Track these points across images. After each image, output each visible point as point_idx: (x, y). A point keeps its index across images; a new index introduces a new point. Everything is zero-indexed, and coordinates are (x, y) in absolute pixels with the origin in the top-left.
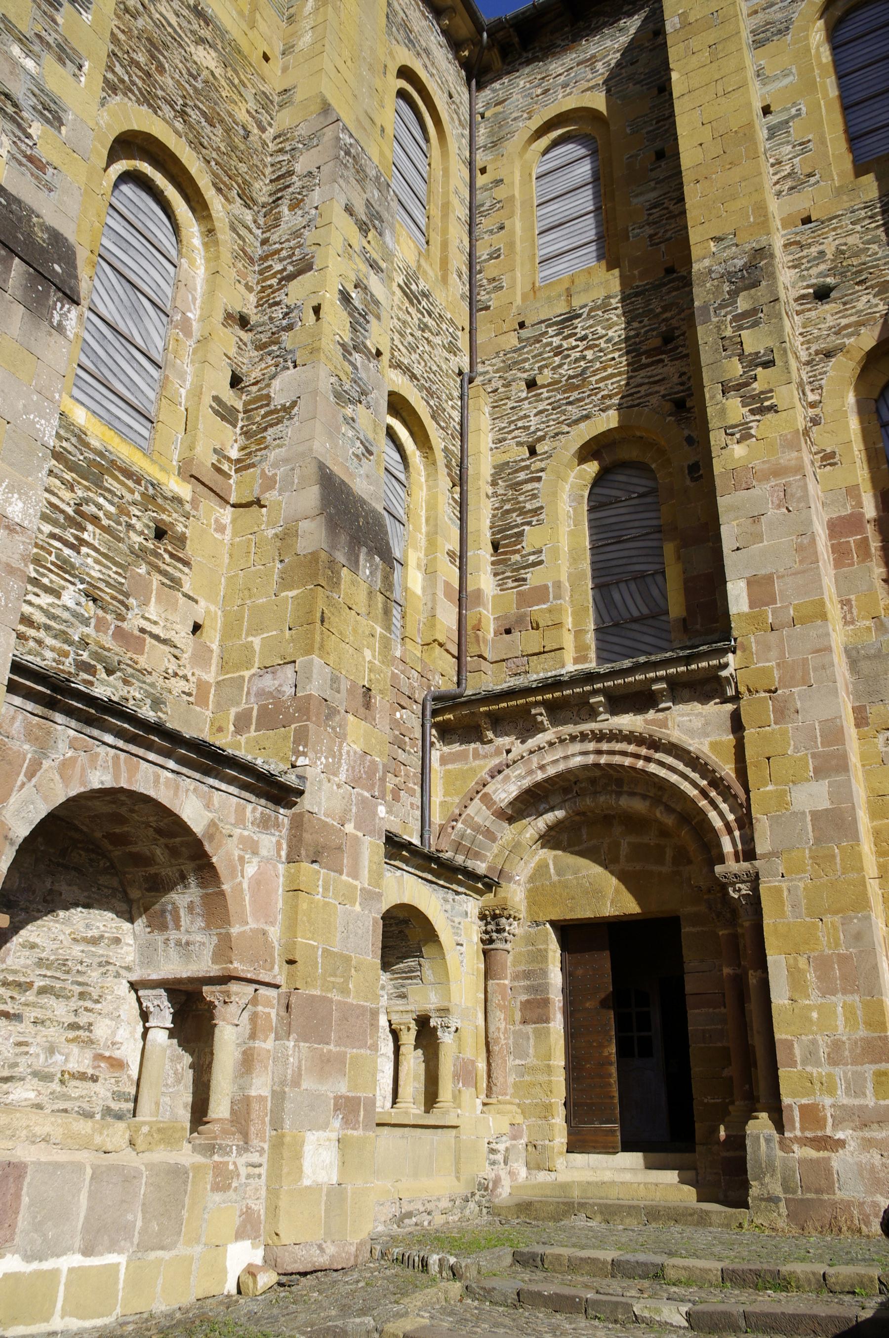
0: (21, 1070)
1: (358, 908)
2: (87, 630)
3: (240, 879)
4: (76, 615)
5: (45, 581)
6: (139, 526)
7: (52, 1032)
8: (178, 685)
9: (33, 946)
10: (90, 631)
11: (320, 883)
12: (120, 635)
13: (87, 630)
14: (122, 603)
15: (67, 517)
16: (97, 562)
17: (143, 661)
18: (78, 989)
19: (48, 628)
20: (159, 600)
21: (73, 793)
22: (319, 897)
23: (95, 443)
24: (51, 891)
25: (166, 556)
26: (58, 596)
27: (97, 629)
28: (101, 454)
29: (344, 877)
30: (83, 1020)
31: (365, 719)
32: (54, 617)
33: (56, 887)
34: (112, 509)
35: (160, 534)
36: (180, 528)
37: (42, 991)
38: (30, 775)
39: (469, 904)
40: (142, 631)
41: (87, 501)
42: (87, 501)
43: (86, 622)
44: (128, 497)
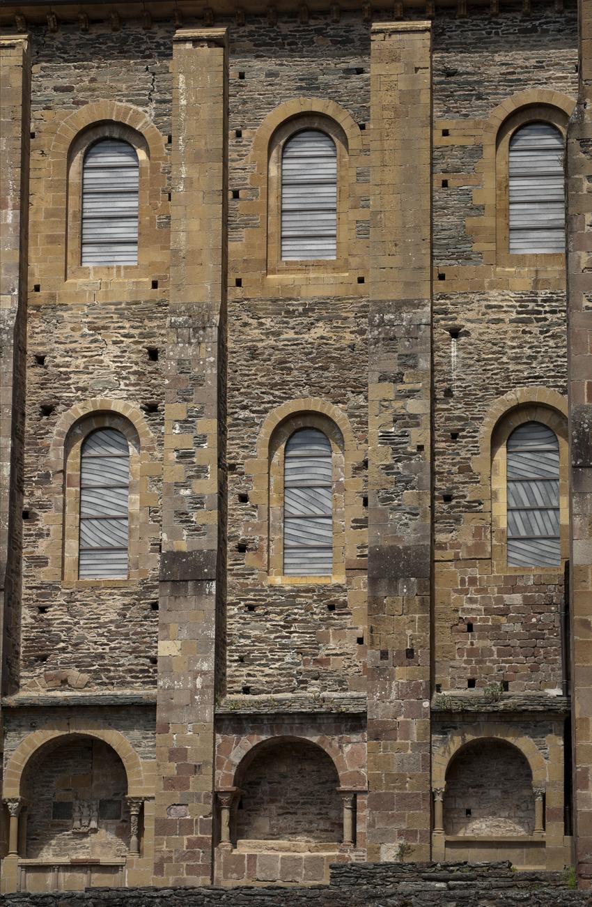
0: (299, 830)
1: (409, 752)
2: (299, 668)
4: (292, 663)
5: (276, 657)
6: (317, 611)
7: (311, 817)
8: (351, 671)
9: (297, 789)
10: (301, 667)
12: (316, 661)
13: (299, 668)
14: (315, 648)
15: (282, 626)
16: (298, 637)
17: (330, 668)
19: (281, 674)
20: (334, 638)
21: (255, 744)
23: (288, 588)
24: (301, 769)
25: (335, 617)
26: (283, 661)
27: (304, 665)
28: (292, 591)
29: (398, 741)
31: (410, 665)
32: (283, 669)
34: (303, 611)
35: (331, 607)
36: (342, 599)
37: (303, 804)
38: (237, 744)
39: (553, 725)
40: (328, 655)
41: (289, 615)
42: (289, 615)
43: (298, 664)
44: (310, 601)
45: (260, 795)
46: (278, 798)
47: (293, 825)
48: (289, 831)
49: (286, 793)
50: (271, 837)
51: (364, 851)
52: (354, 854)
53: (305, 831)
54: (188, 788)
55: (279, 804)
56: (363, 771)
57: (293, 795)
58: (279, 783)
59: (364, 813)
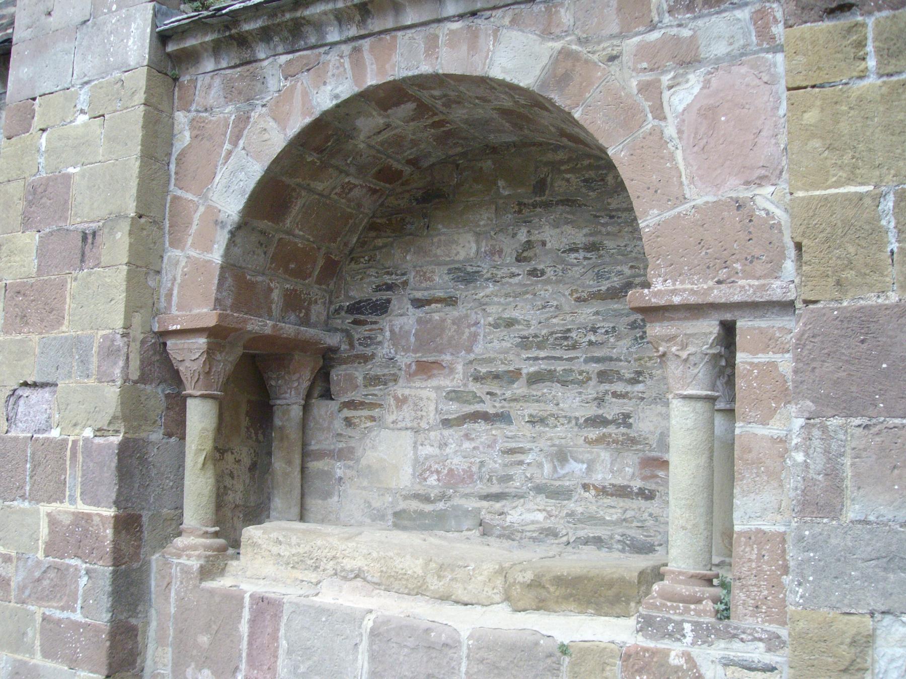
3: (651, 122)
7: (560, 433)
9: (510, 323)
11: (870, 48)
18: (595, 367)
22: (872, 80)
24: (529, 245)
30: (612, 410)
33: (536, 237)
37: (535, 379)
45: (385, 350)
46: (447, 358)
47: (495, 462)
48: (481, 487)
49: (474, 337)
50: (415, 505)
51: (773, 642)
52: (720, 649)
53: (539, 489)
54: (59, 321)
55: (447, 383)
56: (768, 200)
57: (494, 347)
58: (450, 301)
59: (774, 429)
